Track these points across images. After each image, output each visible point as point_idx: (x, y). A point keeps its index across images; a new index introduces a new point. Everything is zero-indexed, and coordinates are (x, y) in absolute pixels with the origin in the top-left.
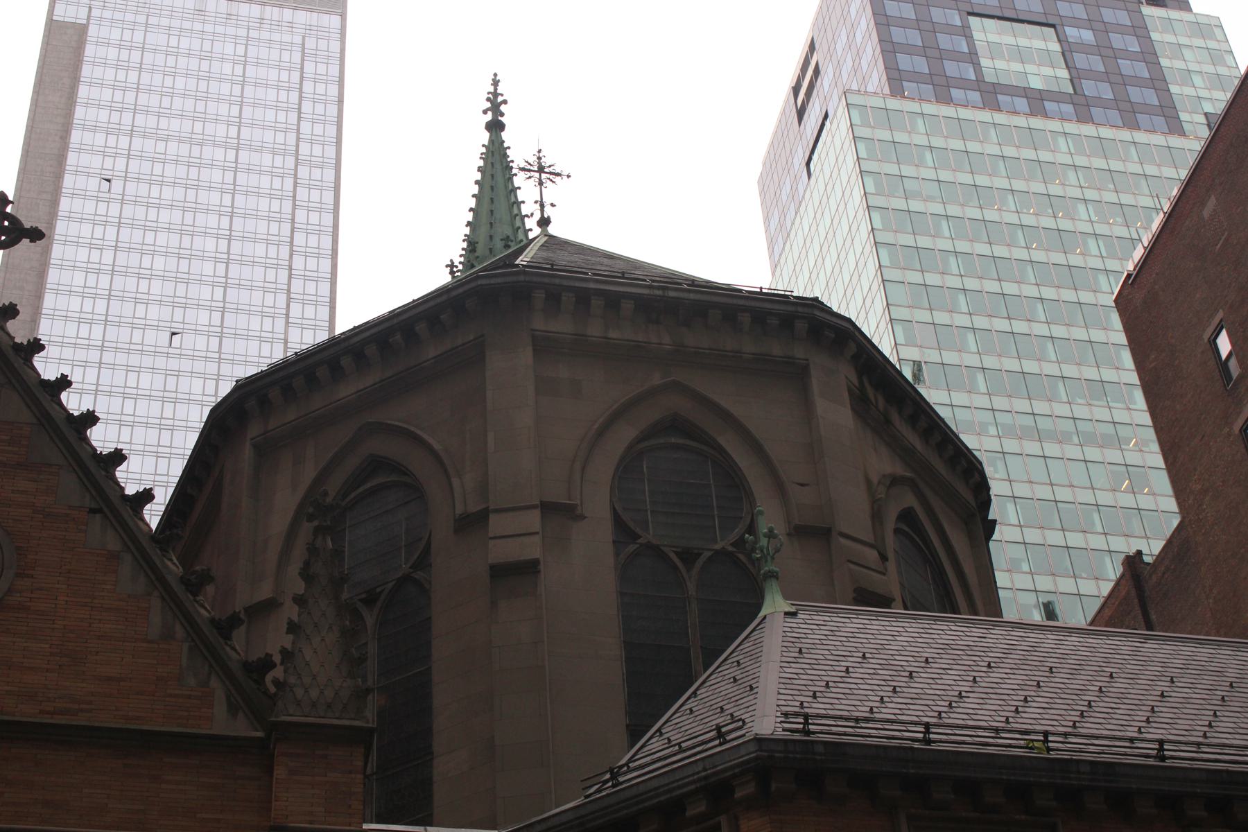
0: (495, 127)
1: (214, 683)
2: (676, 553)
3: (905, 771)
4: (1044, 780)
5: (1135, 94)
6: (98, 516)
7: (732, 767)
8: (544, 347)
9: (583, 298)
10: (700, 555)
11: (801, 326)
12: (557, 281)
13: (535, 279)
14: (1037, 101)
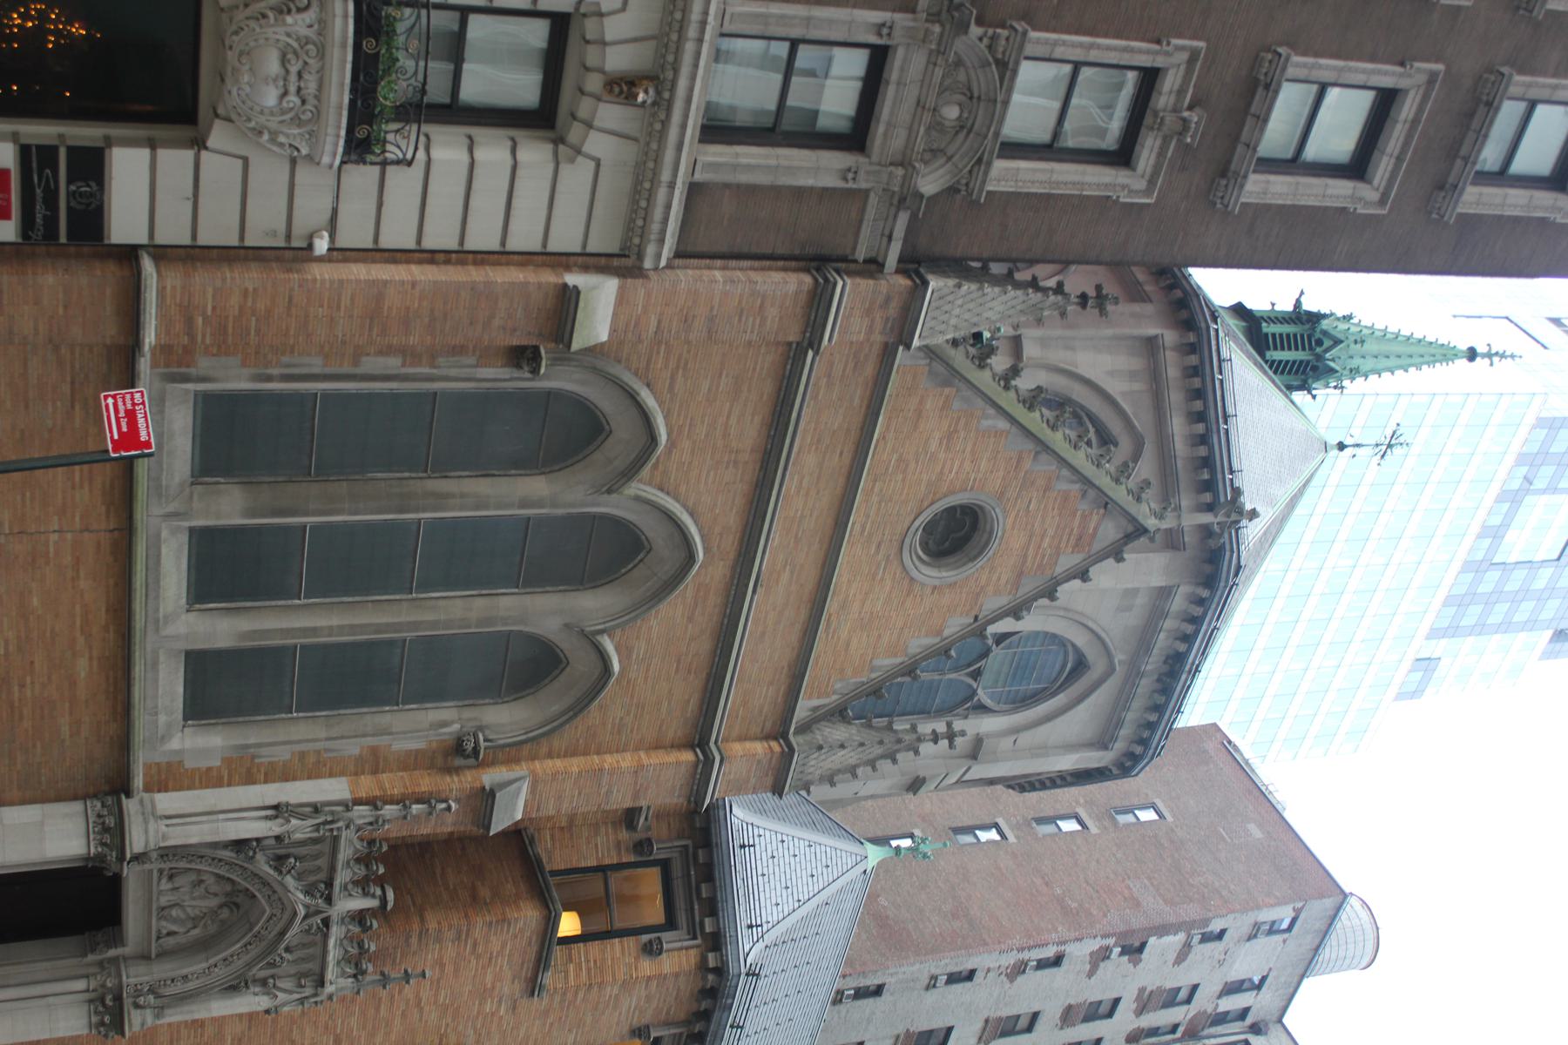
0: (1472, 354)
1: (835, 697)
5: (1475, 610)
7: (727, 956)
8: (1165, 593)
9: (1196, 621)
10: (976, 680)
11: (1138, 750)
12: (1213, 606)
13: (1219, 593)
14: (1495, 534)
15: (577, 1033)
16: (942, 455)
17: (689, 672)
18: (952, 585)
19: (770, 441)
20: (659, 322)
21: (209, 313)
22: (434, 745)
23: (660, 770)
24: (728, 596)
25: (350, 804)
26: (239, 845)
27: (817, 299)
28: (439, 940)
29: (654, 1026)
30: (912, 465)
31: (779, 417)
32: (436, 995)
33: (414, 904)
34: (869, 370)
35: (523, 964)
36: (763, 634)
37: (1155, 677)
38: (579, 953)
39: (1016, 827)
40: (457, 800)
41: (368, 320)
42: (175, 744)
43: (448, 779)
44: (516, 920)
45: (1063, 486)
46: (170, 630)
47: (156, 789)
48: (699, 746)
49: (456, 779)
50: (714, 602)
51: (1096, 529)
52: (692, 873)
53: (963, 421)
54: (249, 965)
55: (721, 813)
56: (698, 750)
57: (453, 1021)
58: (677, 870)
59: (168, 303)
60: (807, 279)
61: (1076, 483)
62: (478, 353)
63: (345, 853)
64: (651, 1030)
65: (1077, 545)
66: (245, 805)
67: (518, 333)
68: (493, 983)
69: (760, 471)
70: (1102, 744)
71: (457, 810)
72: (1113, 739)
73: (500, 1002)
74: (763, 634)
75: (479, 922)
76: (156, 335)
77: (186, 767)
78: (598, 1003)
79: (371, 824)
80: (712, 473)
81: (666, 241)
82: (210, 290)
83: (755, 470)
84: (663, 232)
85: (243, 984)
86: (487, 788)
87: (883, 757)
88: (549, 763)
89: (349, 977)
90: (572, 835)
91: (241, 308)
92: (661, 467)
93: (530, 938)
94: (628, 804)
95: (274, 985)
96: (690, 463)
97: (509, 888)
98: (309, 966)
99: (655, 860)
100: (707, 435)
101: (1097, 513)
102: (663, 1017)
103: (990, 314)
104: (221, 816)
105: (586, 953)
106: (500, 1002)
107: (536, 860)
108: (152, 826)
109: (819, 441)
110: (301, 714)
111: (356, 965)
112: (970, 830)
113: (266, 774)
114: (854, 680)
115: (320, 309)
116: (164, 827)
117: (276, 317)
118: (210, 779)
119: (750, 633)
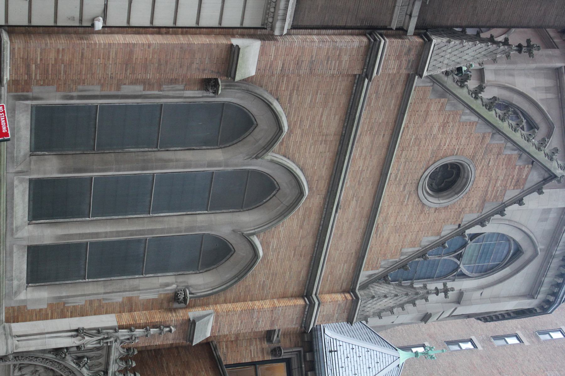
1: (381, 270)
2: (461, 253)
6: (457, 227)
11: (552, 299)
16: (440, 136)
17: (301, 256)
18: (446, 208)
19: (345, 129)
20: (283, 64)
21: (39, 63)
22: (162, 296)
23: (286, 309)
24: (322, 215)
25: (117, 329)
26: (57, 351)
27: (370, 50)
30: (423, 141)
31: (349, 116)
34: (399, 89)
36: (341, 235)
37: (561, 258)
39: (482, 341)
40: (175, 326)
41: (125, 65)
42: (22, 296)
43: (170, 315)
45: (508, 152)
46: (19, 235)
47: (12, 321)
48: (306, 296)
49: (174, 315)
50: (314, 218)
51: (527, 176)
52: (303, 366)
53: (452, 116)
55: (319, 333)
56: (306, 299)
58: (295, 365)
59: (16, 57)
60: (365, 40)
61: (515, 150)
62: (184, 83)
63: (114, 355)
65: (516, 185)
66: (60, 329)
67: (206, 72)
69: (339, 145)
70: (531, 295)
71: (175, 332)
72: (537, 292)
74: (341, 235)
76: (10, 75)
77: (28, 309)
79: (128, 339)
80: (313, 147)
81: (287, 20)
82: (39, 50)
83: (336, 145)
84: (285, 15)
86: (191, 319)
87: (408, 302)
88: (225, 306)
90: (237, 345)
91: (56, 59)
92: (285, 145)
94: (268, 328)
96: (301, 142)
99: (282, 359)
100: (310, 126)
101: (528, 167)
103: (466, 57)
104: (47, 335)
107: (218, 358)
108: (10, 341)
109: (371, 128)
110: (90, 280)
112: (456, 343)
113: (71, 312)
114: (391, 260)
115: (99, 60)
116: (16, 341)
117: (75, 64)
118: (41, 315)
119: (334, 234)
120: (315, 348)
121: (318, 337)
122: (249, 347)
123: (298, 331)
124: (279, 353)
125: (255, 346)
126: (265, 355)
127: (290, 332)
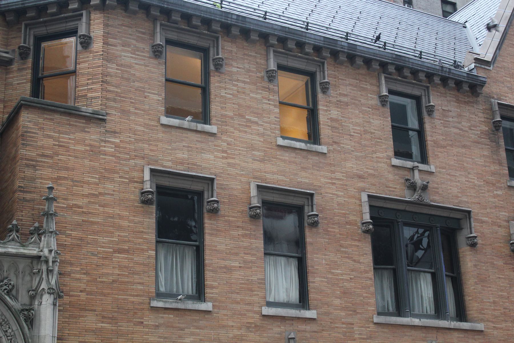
3: (163, 5)
4: (217, 19)
15: (149, 93)
28: (33, 179)
29: (154, 43)
32: (88, 183)
33: (12, 198)
35: (70, 125)
38: (82, 90)
44: (23, 127)
54: (9, 308)
57: (118, 173)
58: (42, 31)
64: (155, 43)
68: (86, 145)
73: (105, 142)
75: (22, 152)
78: (122, 77)
85: (26, 313)
89: (40, 240)
93: (45, 119)
95: (33, 290)
97: (14, 135)
98: (21, 267)
102: (146, 37)
105: (83, 86)
106: (105, 142)
111: (32, 234)
120: (20, 6)
121: (8, 4)
122: (14, 86)
123: (5, 29)
124: (22, 50)
125: (14, 79)
126: (26, 66)
127: (3, 38)
